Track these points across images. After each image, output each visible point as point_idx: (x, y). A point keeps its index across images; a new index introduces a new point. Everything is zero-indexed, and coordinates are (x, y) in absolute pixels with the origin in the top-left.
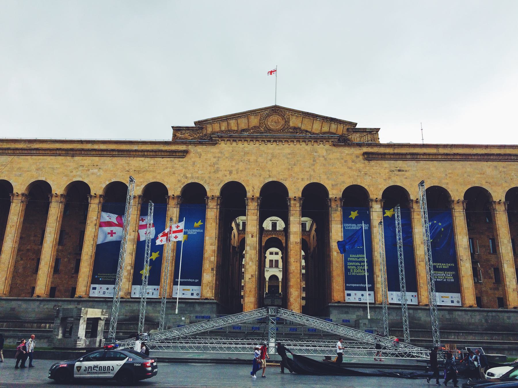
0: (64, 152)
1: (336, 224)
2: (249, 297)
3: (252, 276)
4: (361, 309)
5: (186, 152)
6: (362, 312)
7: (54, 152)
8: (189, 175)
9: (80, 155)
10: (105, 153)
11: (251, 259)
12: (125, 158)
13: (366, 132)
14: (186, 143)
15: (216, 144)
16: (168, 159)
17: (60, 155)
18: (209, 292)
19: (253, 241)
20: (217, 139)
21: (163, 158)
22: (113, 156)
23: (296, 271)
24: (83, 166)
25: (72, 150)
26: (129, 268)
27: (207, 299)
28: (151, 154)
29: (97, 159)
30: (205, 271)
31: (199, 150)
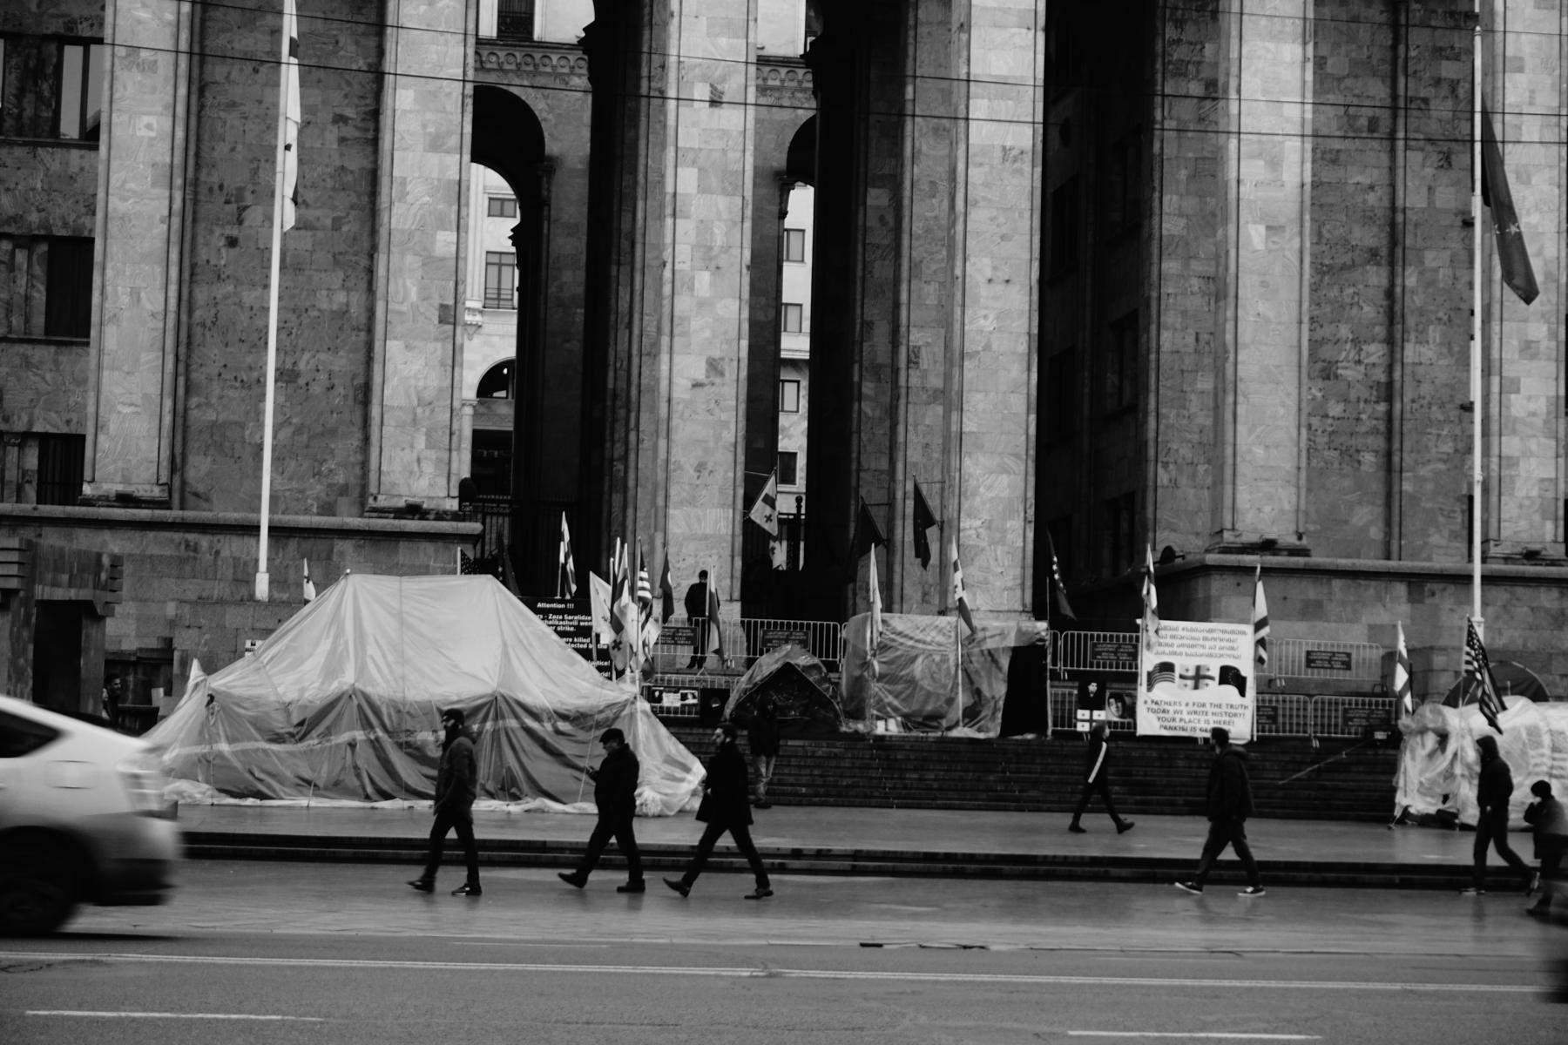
1: (1276, 37)
2: (692, 501)
3: (714, 366)
4: (1401, 589)
6: (1404, 608)
11: (708, 257)
18: (428, 468)
19: (724, 133)
23: (1000, 344)
27: (414, 511)
30: (397, 328)
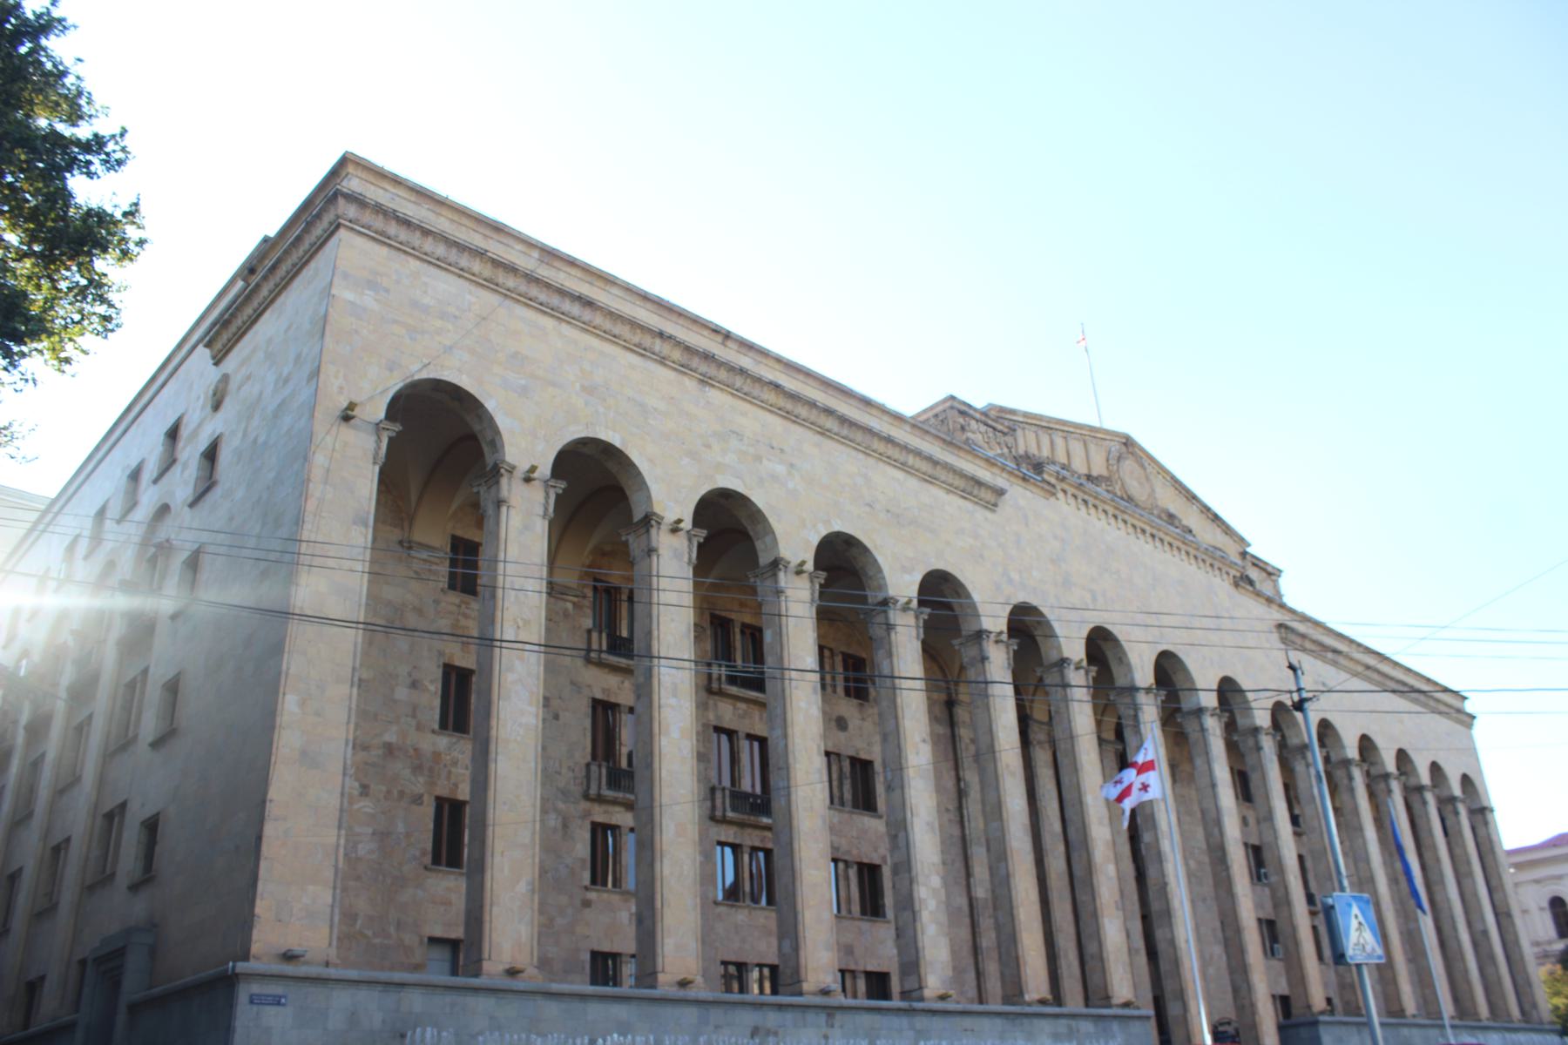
0: (677, 355)
5: (1000, 492)
7: (647, 341)
8: (1015, 576)
9: (728, 387)
10: (803, 411)
12: (854, 453)
13: (1264, 570)
14: (994, 465)
15: (1054, 494)
16: (961, 502)
17: (662, 361)
20: (1053, 481)
21: (949, 492)
22: (824, 432)
24: (740, 436)
25: (708, 357)
26: (936, 881)
28: (925, 466)
29: (776, 423)
31: (1022, 502)
